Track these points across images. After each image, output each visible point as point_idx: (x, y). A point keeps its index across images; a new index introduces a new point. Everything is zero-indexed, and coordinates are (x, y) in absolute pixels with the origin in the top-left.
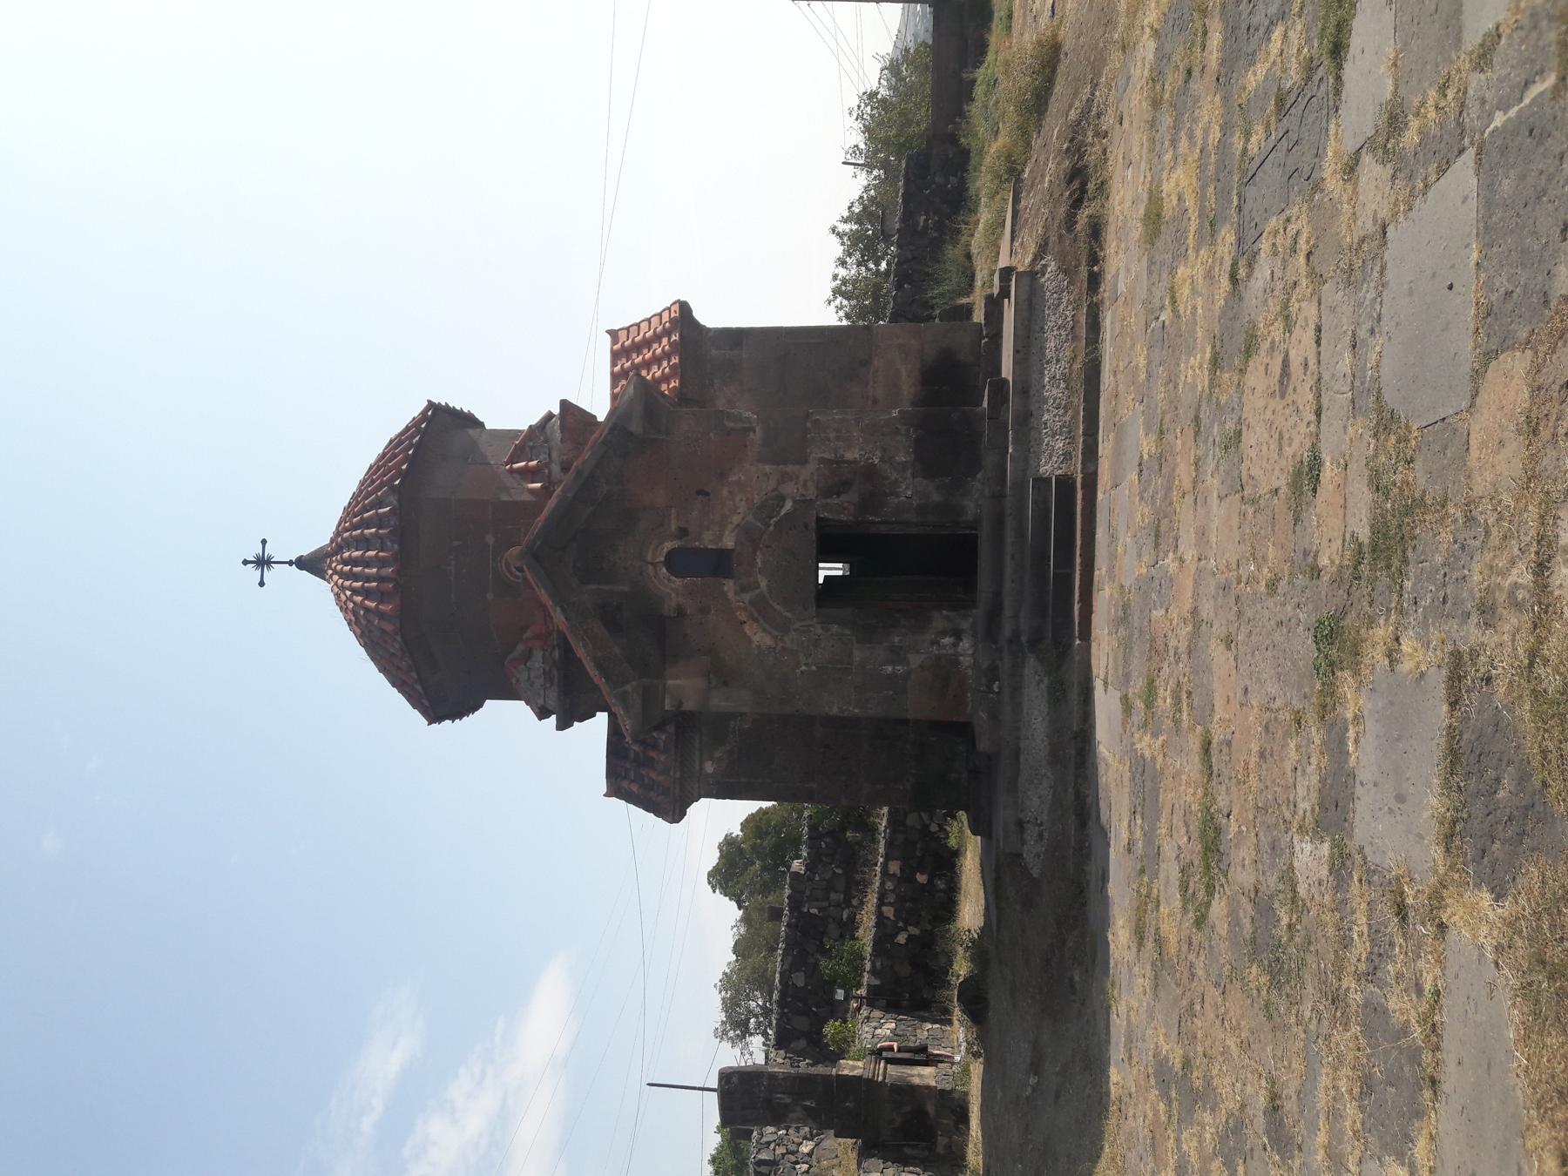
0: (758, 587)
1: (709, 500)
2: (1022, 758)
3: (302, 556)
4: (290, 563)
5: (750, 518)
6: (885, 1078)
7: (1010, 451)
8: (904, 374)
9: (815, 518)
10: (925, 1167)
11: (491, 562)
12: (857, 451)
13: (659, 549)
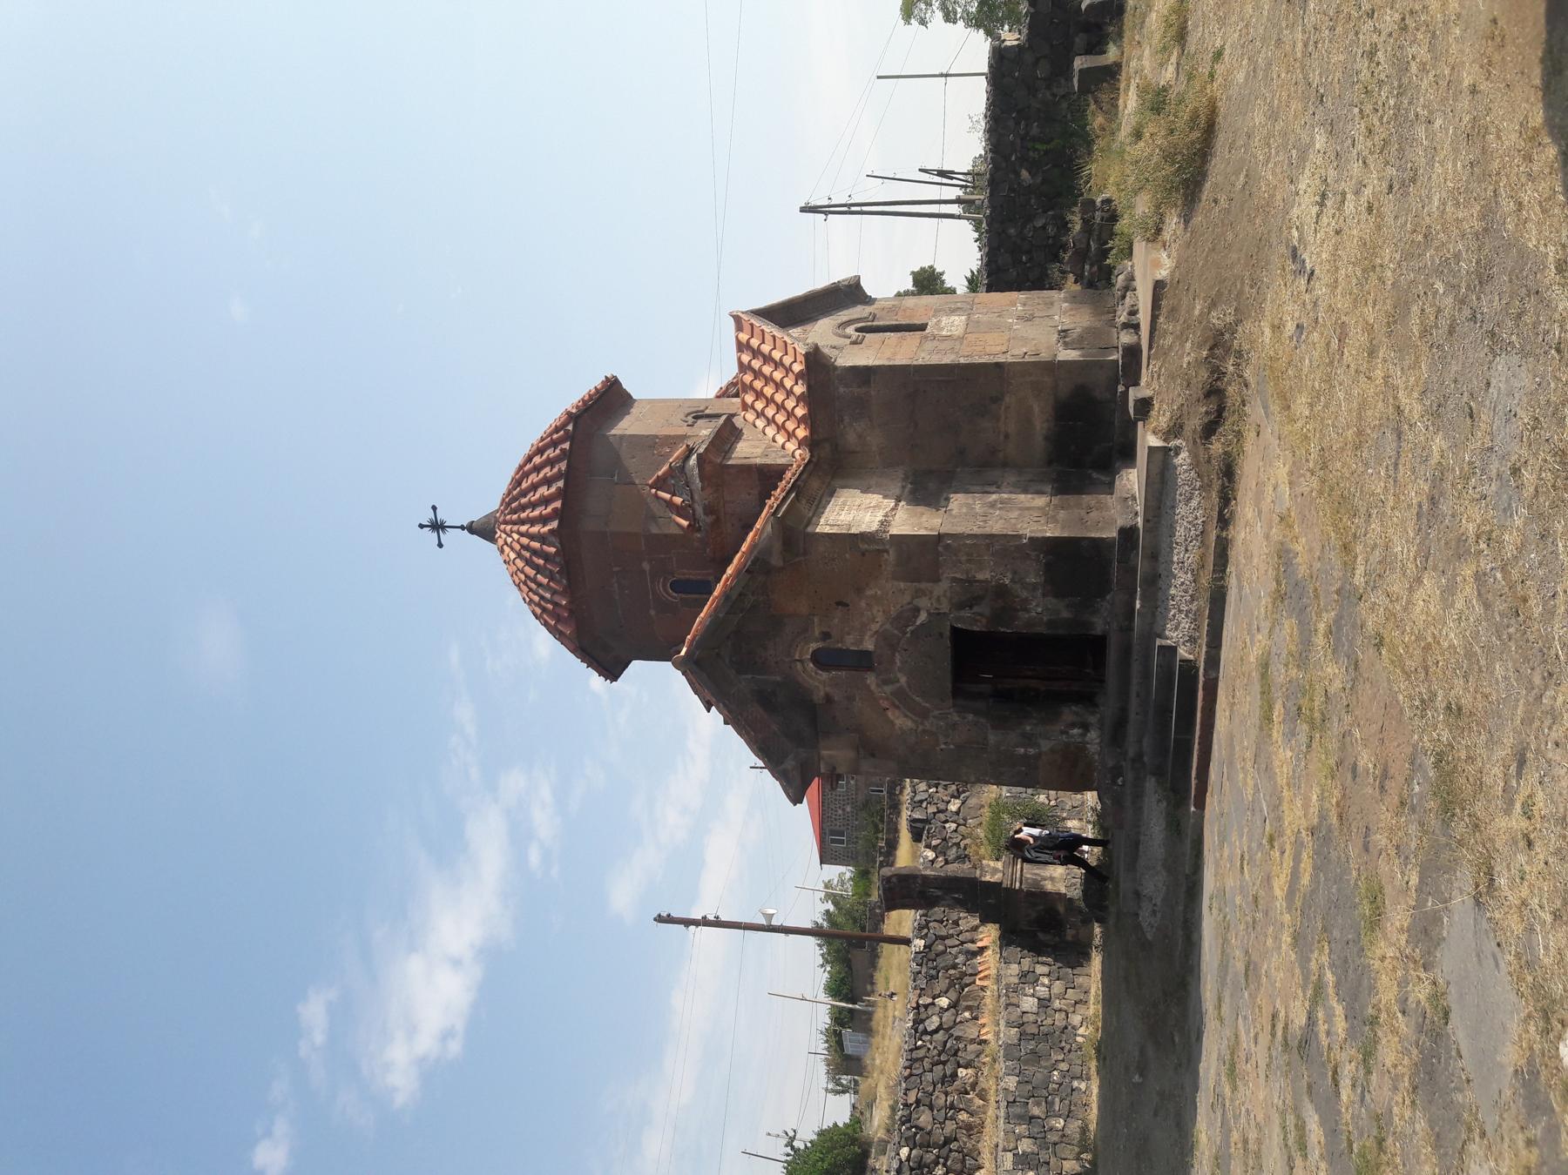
0: (898, 681)
1: (848, 610)
2: (1141, 846)
3: (473, 522)
4: (462, 528)
5: (888, 626)
6: (1021, 884)
7: (1138, 606)
8: (1036, 409)
9: (949, 628)
10: (1056, 956)
11: (649, 584)
12: (988, 572)
13: (805, 648)
